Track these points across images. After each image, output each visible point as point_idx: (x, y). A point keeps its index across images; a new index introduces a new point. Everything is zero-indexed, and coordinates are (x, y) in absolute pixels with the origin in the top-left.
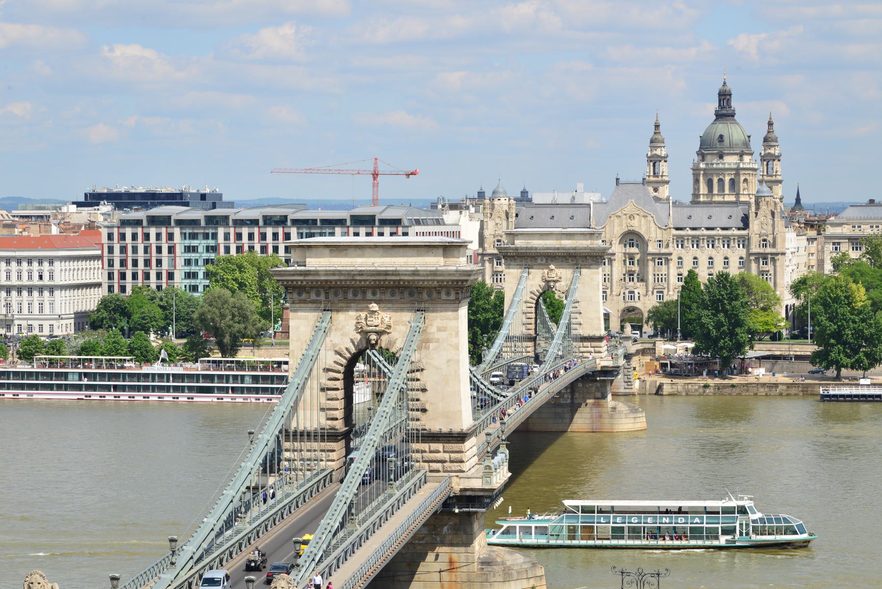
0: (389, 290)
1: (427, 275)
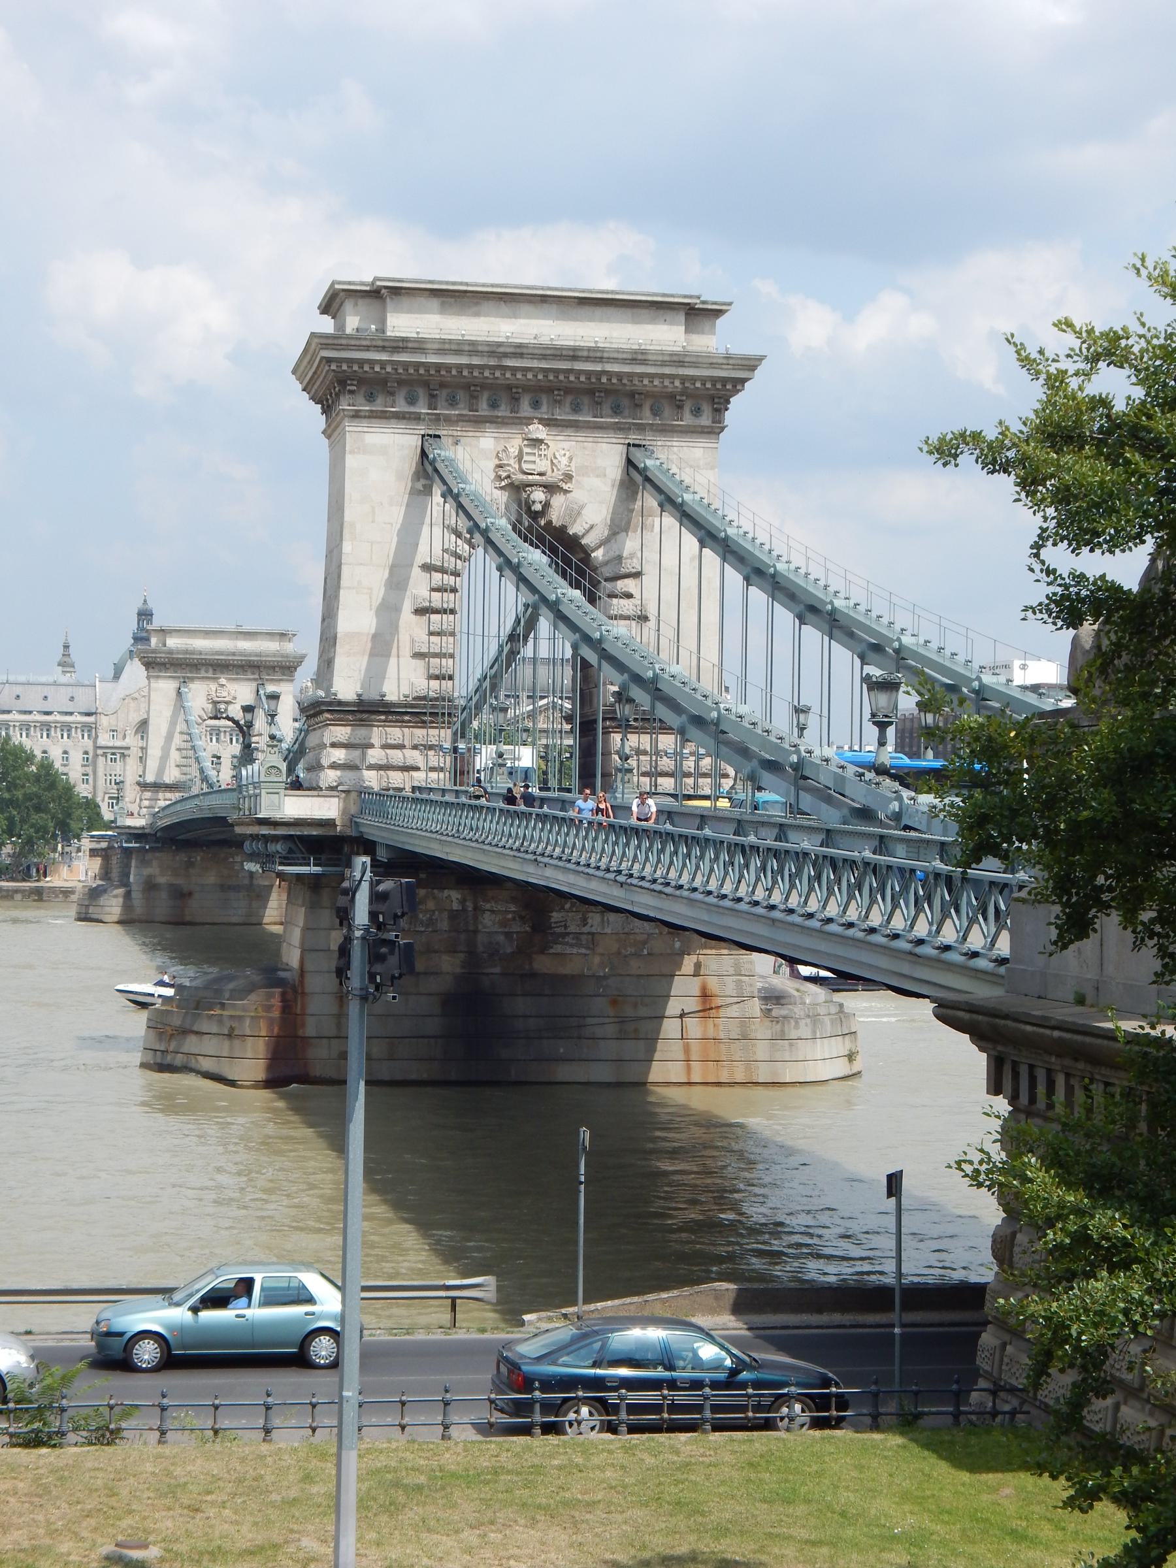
0: (569, 399)
1: (663, 364)
